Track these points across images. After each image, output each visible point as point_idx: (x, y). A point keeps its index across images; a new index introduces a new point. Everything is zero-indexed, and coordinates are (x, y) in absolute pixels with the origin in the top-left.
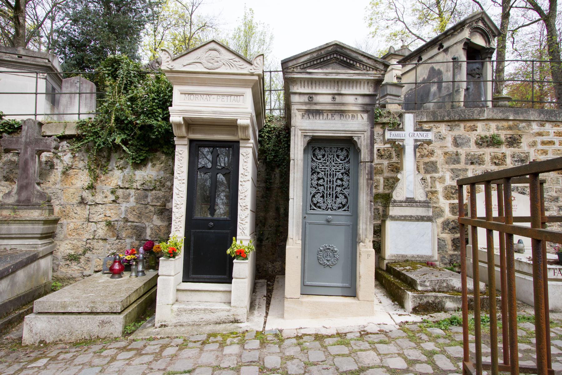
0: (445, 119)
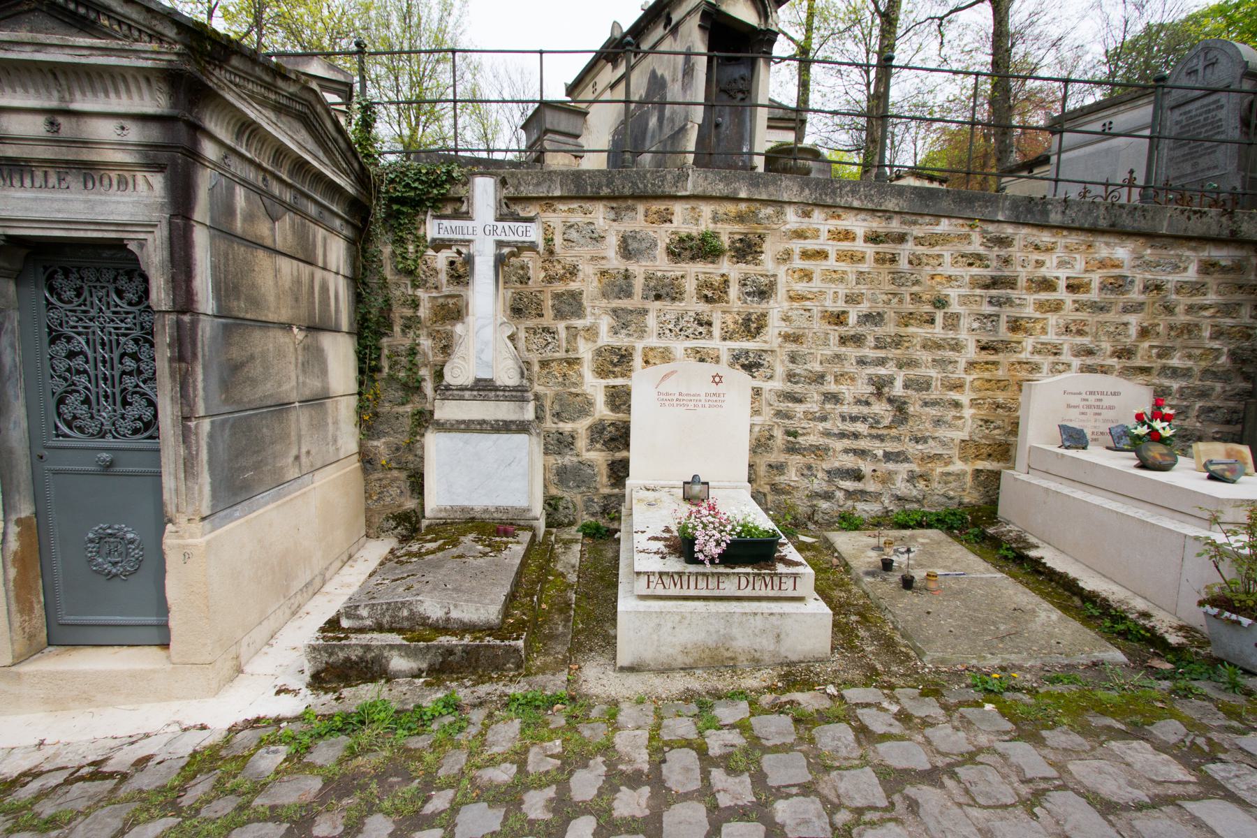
0: (602, 194)
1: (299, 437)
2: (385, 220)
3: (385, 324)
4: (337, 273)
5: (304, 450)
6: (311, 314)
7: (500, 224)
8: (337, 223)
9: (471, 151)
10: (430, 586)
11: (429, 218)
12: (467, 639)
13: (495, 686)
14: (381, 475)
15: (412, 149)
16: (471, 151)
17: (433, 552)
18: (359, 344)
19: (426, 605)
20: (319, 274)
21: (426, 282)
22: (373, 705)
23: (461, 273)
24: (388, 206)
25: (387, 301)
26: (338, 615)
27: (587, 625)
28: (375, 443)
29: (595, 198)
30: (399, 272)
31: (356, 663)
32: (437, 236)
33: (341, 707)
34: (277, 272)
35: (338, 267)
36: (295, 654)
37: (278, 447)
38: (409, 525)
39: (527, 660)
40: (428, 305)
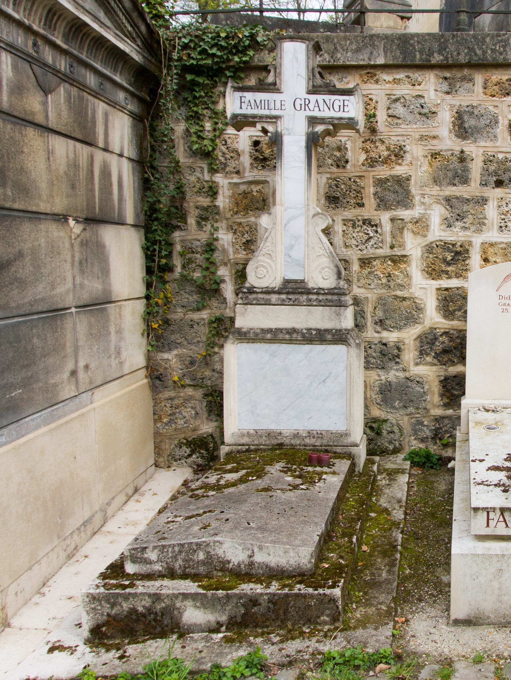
0: (433, 62)
1: (76, 349)
2: (177, 93)
3: (177, 216)
4: (121, 155)
5: (81, 364)
6: (90, 205)
7: (313, 98)
8: (121, 96)
9: (279, 11)
10: (230, 524)
11: (229, 90)
12: (274, 587)
13: (307, 643)
14: (172, 394)
15: (209, 8)
16: (279, 11)
17: (234, 484)
18: (147, 239)
19: (225, 546)
20: (99, 156)
21: (226, 165)
22: (163, 665)
23: (268, 153)
24: (181, 76)
25: (180, 188)
26: (122, 559)
27: (416, 570)
28: (166, 356)
29: (426, 66)
30: (194, 154)
31: (144, 615)
32: (238, 111)
33: (125, 667)
34: (50, 153)
35: (122, 148)
36: (72, 604)
37: (51, 360)
38: (205, 452)
39: (345, 611)
40: (228, 193)
